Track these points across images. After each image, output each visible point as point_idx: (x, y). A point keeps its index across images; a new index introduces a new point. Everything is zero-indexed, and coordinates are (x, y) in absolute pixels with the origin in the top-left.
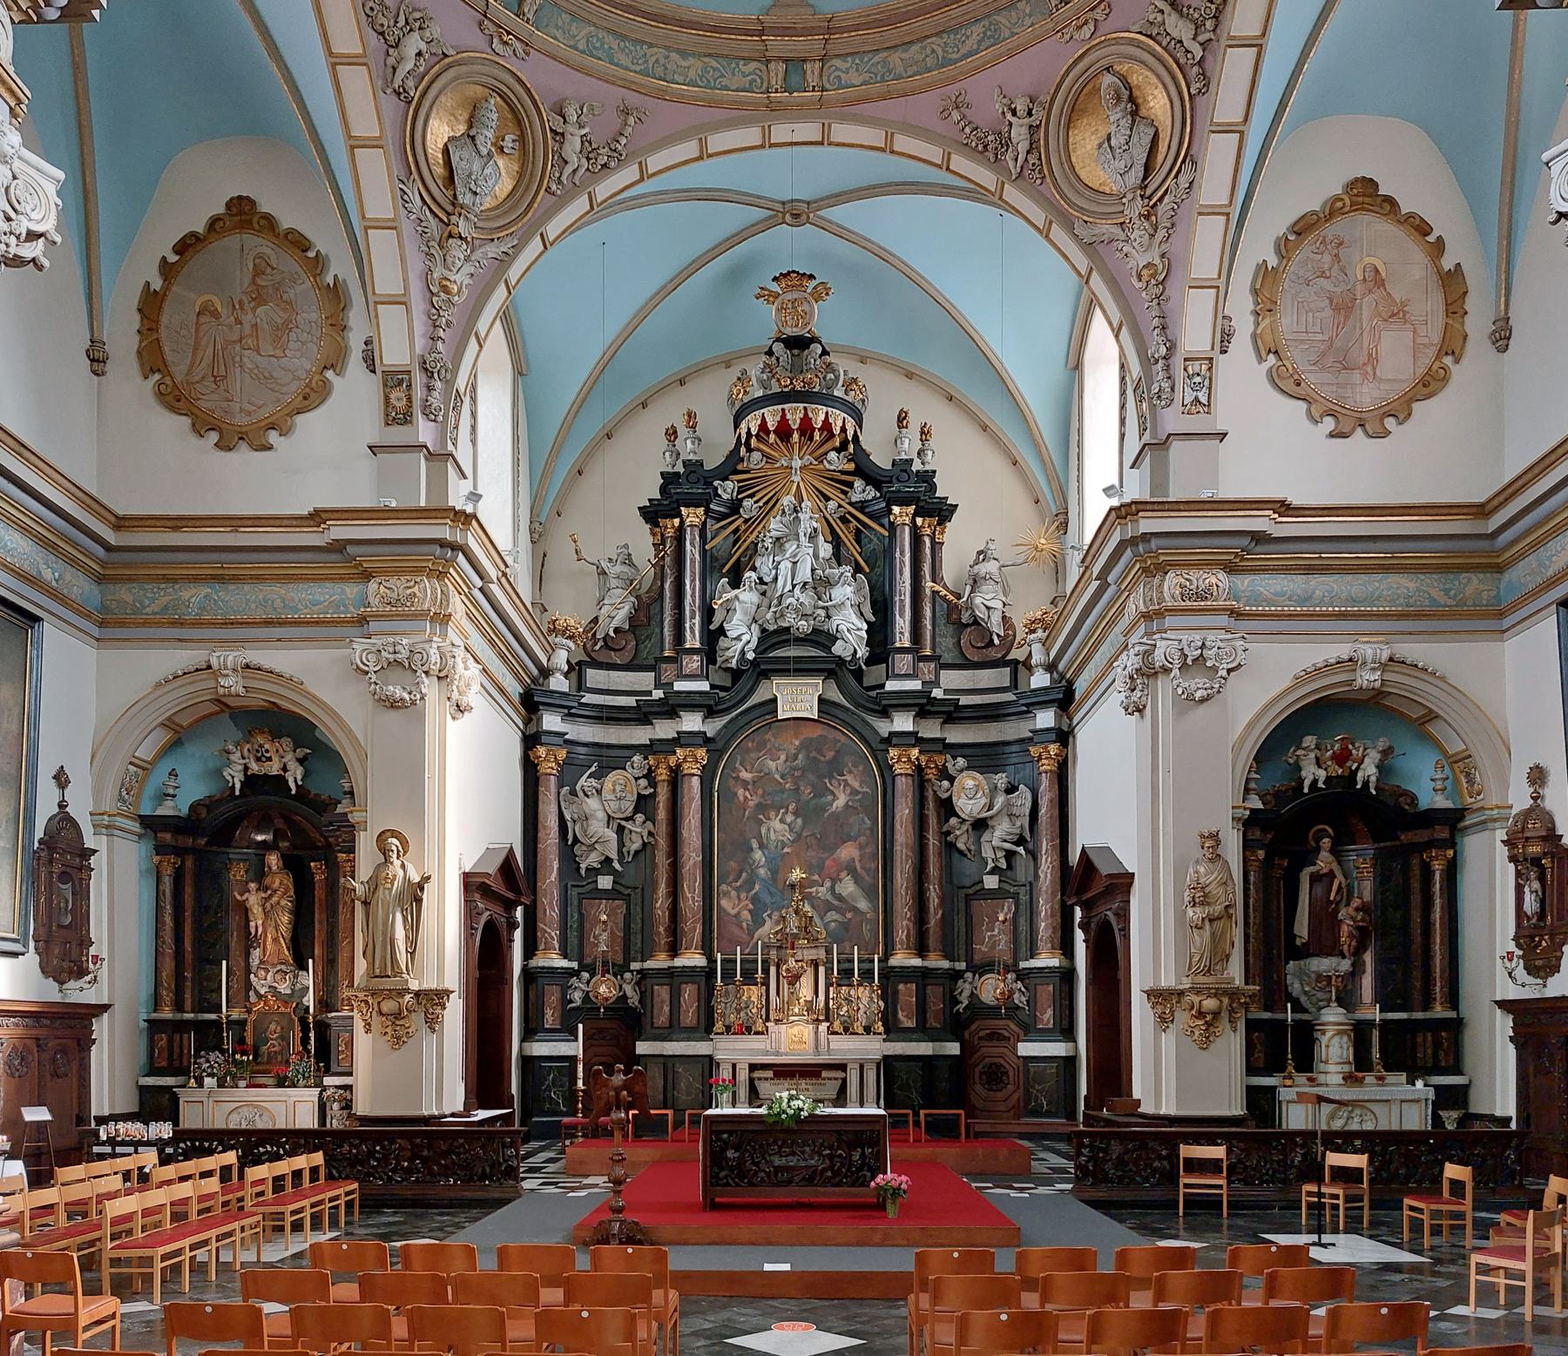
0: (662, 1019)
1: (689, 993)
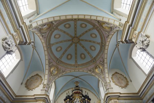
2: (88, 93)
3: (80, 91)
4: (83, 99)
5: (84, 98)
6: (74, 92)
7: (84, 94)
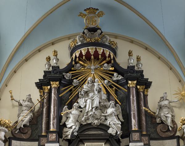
2: (138, 59)
3: (107, 52)
4: (117, 82)
5: (120, 77)
6: (77, 53)
7: (123, 61)
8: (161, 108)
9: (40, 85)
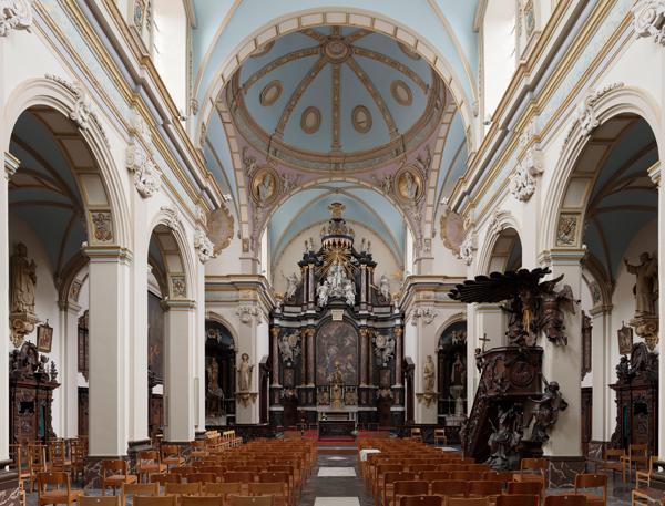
0: (304, 401)
1: (310, 394)
2: (369, 244)
3: (348, 241)
6: (326, 242)
8: (382, 284)
9: (301, 264)
